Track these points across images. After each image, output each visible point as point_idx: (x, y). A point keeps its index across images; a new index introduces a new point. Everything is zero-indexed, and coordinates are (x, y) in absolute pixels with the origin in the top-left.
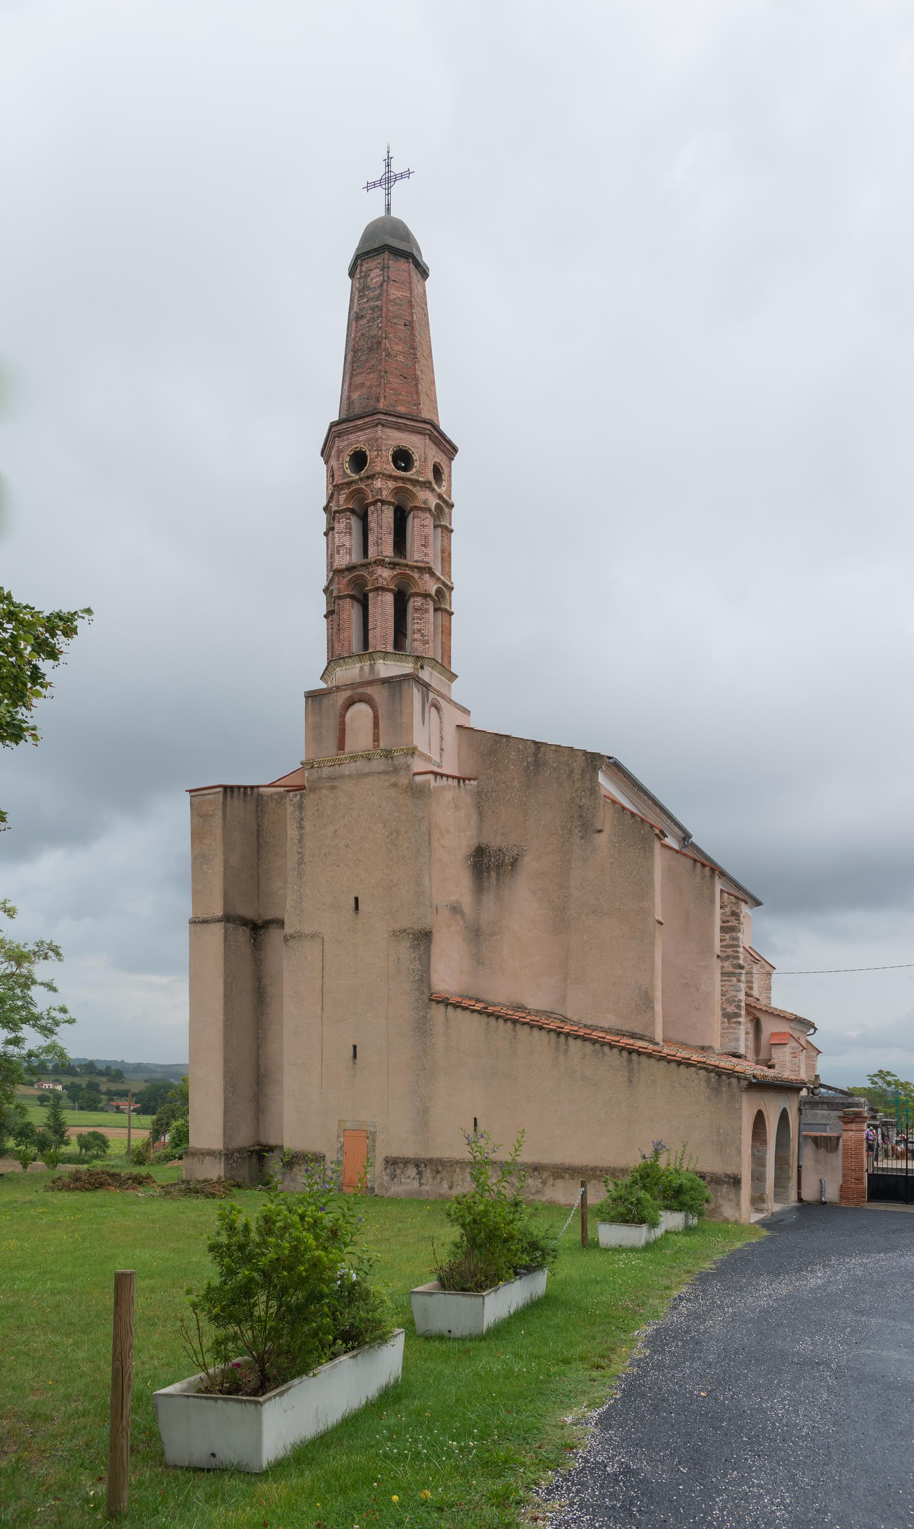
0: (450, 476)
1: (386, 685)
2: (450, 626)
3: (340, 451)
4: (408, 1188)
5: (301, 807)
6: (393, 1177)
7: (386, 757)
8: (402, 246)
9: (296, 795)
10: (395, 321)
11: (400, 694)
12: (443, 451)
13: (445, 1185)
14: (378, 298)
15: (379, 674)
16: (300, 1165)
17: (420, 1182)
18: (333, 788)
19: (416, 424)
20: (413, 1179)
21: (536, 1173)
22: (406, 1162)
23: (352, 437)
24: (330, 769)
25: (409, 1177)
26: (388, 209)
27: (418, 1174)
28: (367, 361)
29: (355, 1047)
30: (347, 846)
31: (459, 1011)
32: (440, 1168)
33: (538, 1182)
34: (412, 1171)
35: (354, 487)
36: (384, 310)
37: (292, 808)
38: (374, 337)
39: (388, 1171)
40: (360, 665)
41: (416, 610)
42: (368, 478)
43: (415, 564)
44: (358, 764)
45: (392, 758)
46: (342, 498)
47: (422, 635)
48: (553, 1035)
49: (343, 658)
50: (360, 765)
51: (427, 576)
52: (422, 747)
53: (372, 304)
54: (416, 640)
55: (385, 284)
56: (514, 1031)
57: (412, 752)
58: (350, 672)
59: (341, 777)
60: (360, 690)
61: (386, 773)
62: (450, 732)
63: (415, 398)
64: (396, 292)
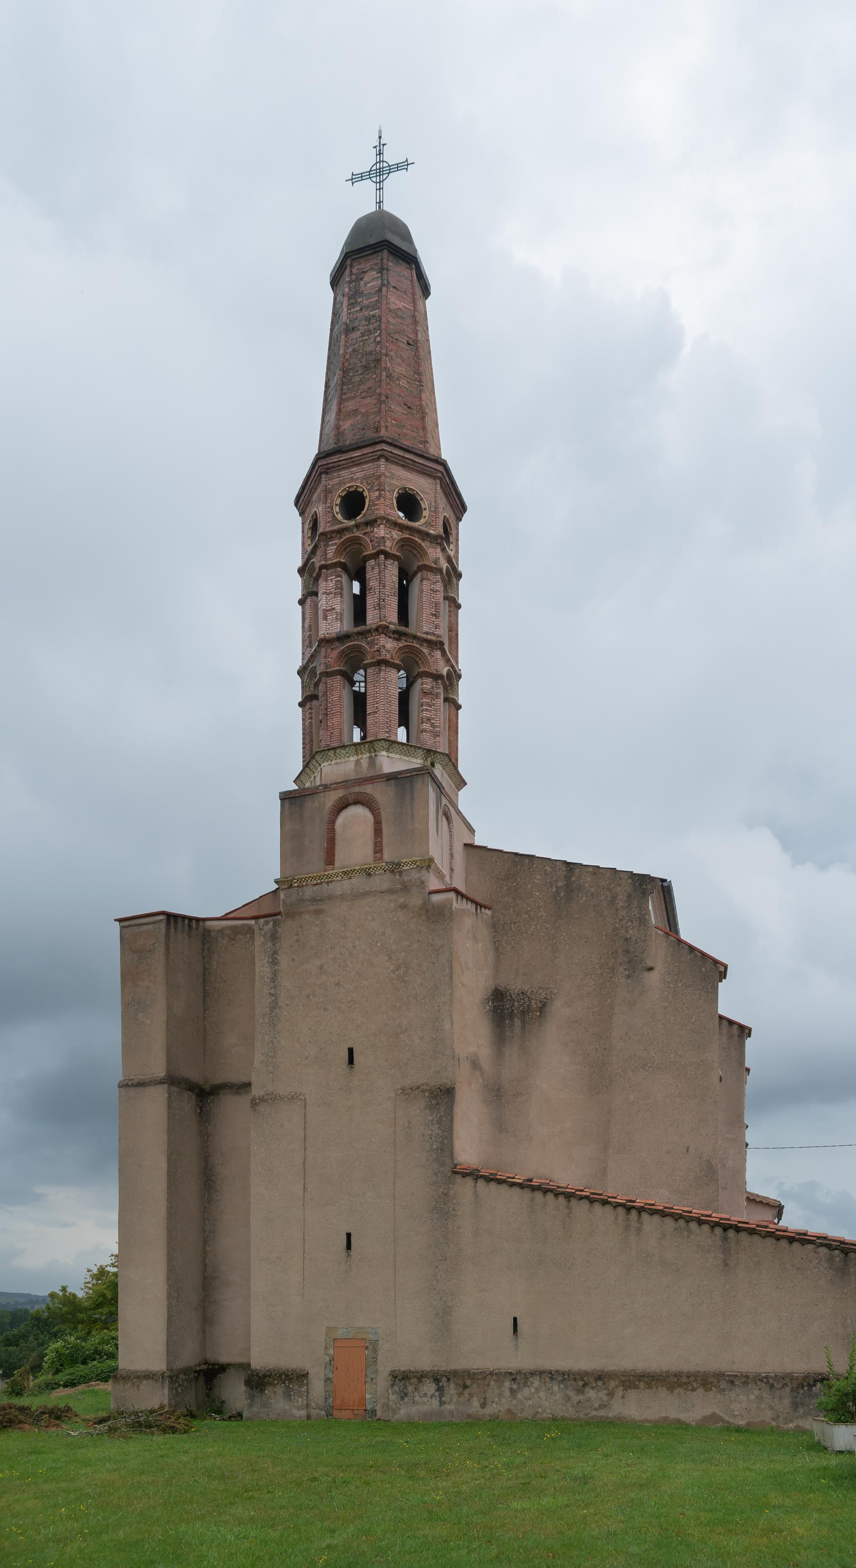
1: (392, 782)
3: (328, 492)
4: (425, 1408)
5: (274, 937)
6: (403, 1395)
7: (392, 872)
8: (404, 246)
9: (267, 923)
10: (397, 336)
11: (412, 793)
13: (476, 1403)
14: (374, 306)
15: (381, 769)
16: (275, 1385)
17: (440, 1401)
18: (318, 912)
19: (426, 463)
20: (431, 1397)
21: (600, 1383)
22: (421, 1376)
23: (345, 474)
24: (315, 888)
25: (425, 1395)
27: (438, 1390)
28: (361, 382)
29: (349, 1235)
30: (338, 984)
31: (493, 1186)
32: (468, 1382)
33: (603, 1394)
34: (429, 1387)
35: (348, 535)
36: (384, 320)
37: (262, 939)
38: (371, 353)
39: (396, 1388)
40: (353, 759)
42: (367, 524)
43: (425, 636)
44: (354, 881)
45: (400, 873)
46: (331, 550)
48: (621, 1211)
49: (334, 749)
50: (358, 882)
52: (441, 862)
53: (366, 313)
54: (425, 731)
55: (384, 289)
56: (569, 1207)
57: (428, 864)
58: (337, 769)
59: (330, 898)
60: (356, 789)
61: (392, 891)
64: (398, 302)
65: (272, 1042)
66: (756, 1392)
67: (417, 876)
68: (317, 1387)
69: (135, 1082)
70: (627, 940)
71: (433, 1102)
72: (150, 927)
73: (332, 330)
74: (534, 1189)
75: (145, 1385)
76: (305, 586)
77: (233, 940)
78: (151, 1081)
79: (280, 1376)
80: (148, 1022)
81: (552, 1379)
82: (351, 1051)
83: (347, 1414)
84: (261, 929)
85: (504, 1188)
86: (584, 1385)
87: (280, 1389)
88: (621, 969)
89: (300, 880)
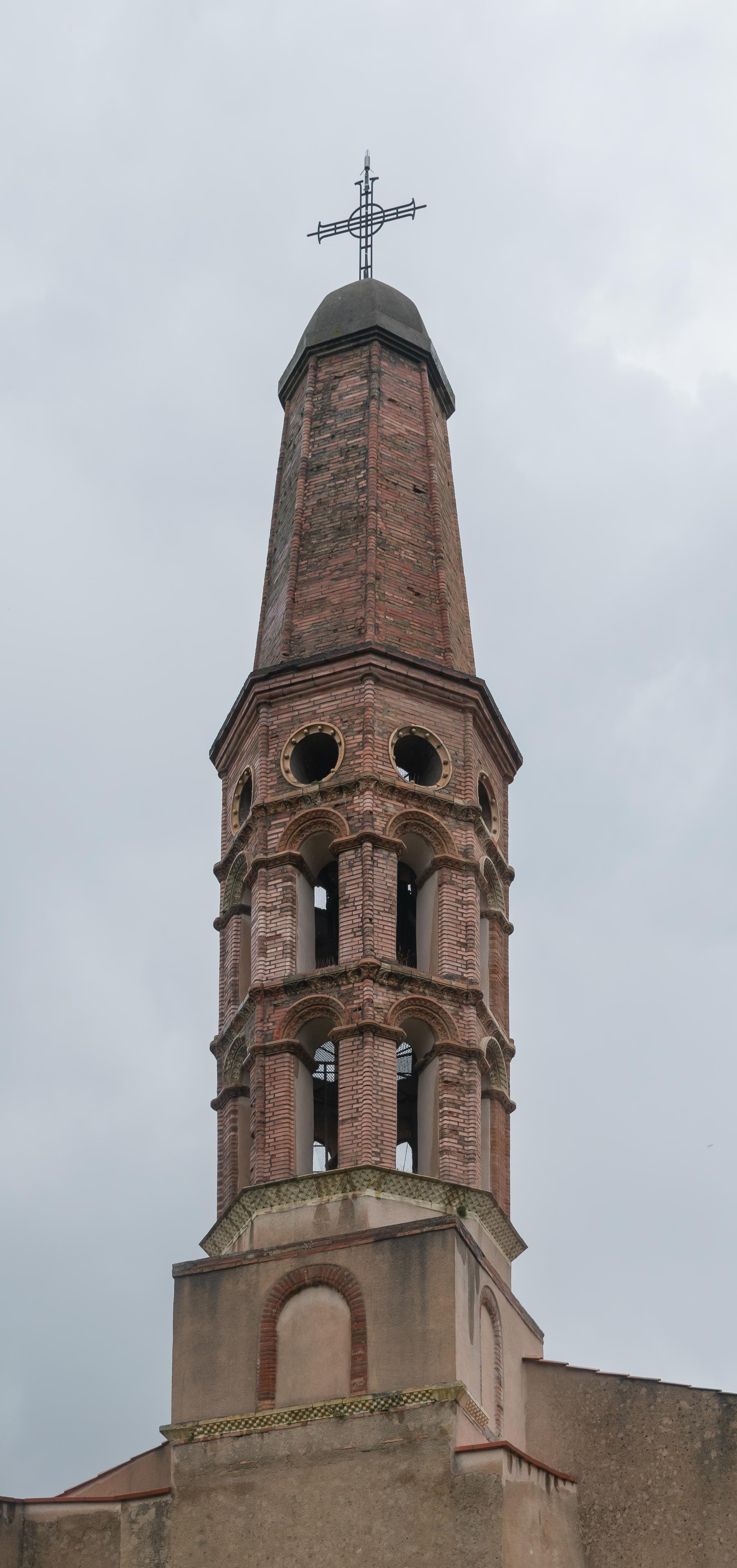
0: (505, 814)
1: (386, 1244)
2: (508, 1136)
3: (270, 736)
5: (157, 1536)
7: (385, 1412)
8: (407, 335)
9: (144, 1510)
10: (395, 478)
11: (423, 1264)
12: (494, 757)
14: (356, 432)
15: (365, 1221)
18: (242, 1489)
19: (448, 685)
23: (302, 705)
24: (238, 1444)
26: (366, 268)
28: (331, 555)
35: (305, 809)
36: (372, 453)
37: (135, 1541)
38: (349, 506)
40: (312, 1203)
41: (448, 1084)
42: (340, 789)
43: (446, 982)
45: (401, 1415)
46: (275, 835)
47: (461, 1141)
49: (277, 1184)
50: (319, 1432)
51: (471, 1013)
52: (478, 1391)
53: (342, 443)
54: (448, 1152)
55: (373, 403)
57: (454, 1398)
58: (281, 1221)
59: (267, 1461)
60: (318, 1258)
61: (383, 1449)
62: (512, 1367)
63: (439, 636)
64: (397, 424)
67: (433, 1420)
73: (281, 470)
76: (226, 897)
77: (80, 1541)
84: (133, 1522)
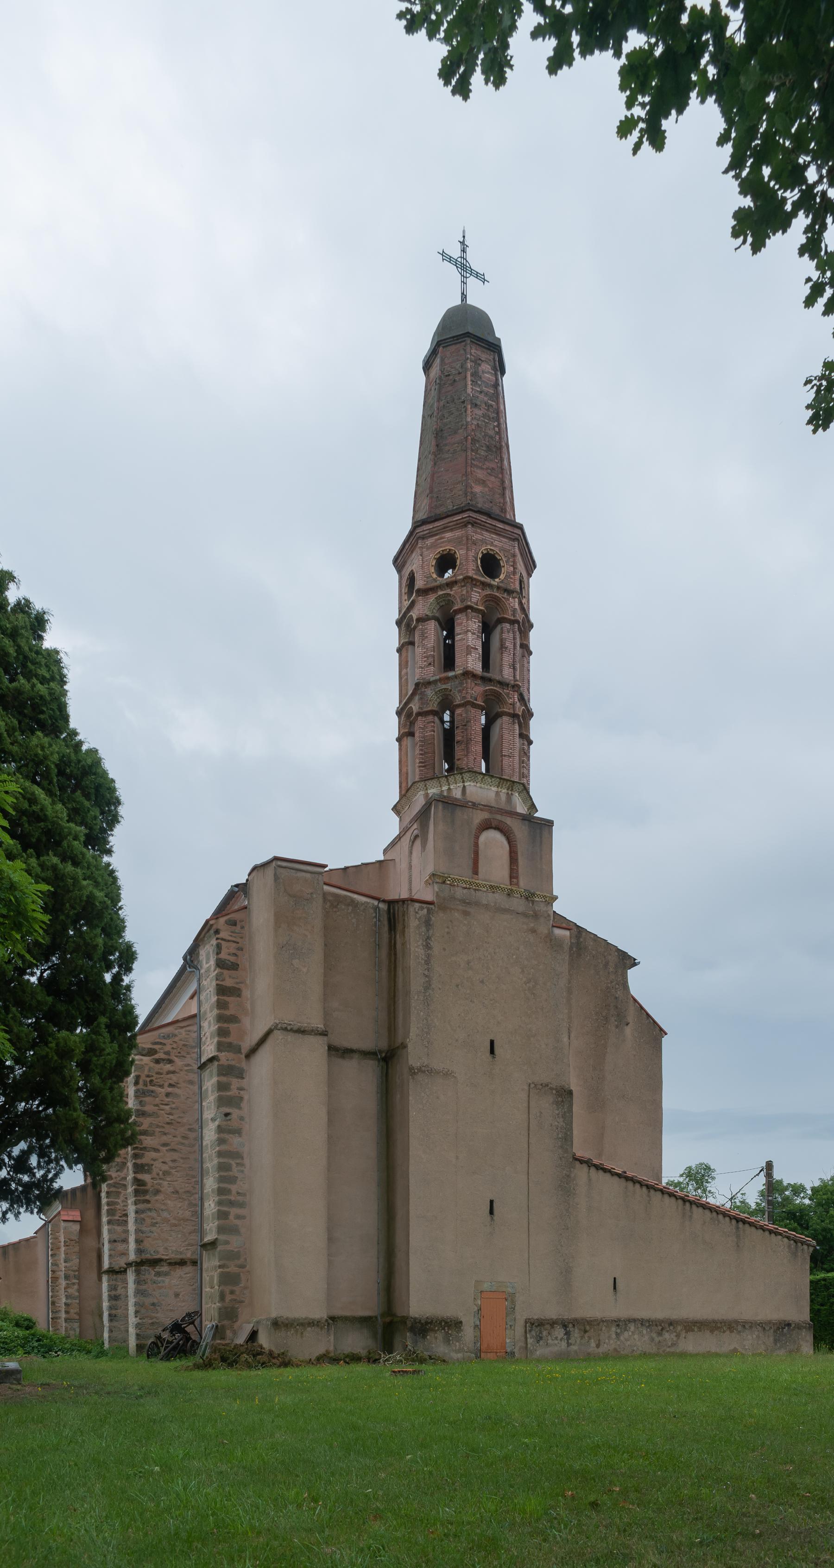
1: (526, 822)
4: (556, 1349)
6: (539, 1338)
9: (422, 909)
11: (541, 837)
13: (593, 1344)
15: (516, 808)
16: (436, 1331)
17: (568, 1343)
20: (561, 1340)
21: (671, 1328)
22: (553, 1323)
24: (465, 891)
25: (556, 1338)
26: (464, 296)
27: (566, 1334)
29: (492, 1202)
30: (482, 982)
31: (601, 1172)
32: (588, 1328)
33: (673, 1336)
34: (559, 1332)
39: (533, 1333)
40: (494, 789)
44: (497, 896)
48: (680, 1202)
56: (649, 1196)
59: (477, 904)
60: (499, 817)
61: (525, 915)
65: (427, 1020)
66: (756, 1333)
67: (545, 909)
68: (468, 1333)
69: (295, 1028)
70: (616, 998)
71: (560, 1099)
72: (308, 875)
74: (627, 1179)
75: (309, 1332)
77: (336, 907)
78: (312, 1031)
79: (440, 1323)
80: (305, 970)
81: (642, 1324)
82: (492, 1043)
83: (491, 1356)
84: (417, 913)
85: (608, 1175)
86: (662, 1329)
87: (440, 1335)
88: (613, 1019)
89: (454, 880)
